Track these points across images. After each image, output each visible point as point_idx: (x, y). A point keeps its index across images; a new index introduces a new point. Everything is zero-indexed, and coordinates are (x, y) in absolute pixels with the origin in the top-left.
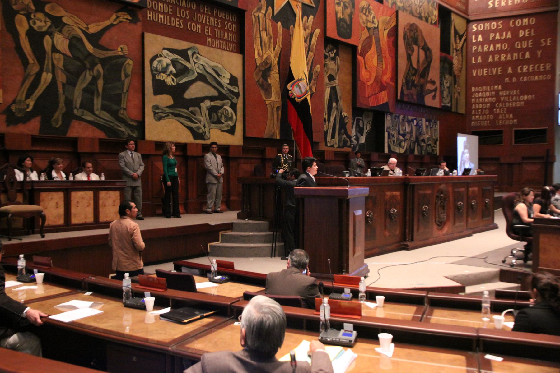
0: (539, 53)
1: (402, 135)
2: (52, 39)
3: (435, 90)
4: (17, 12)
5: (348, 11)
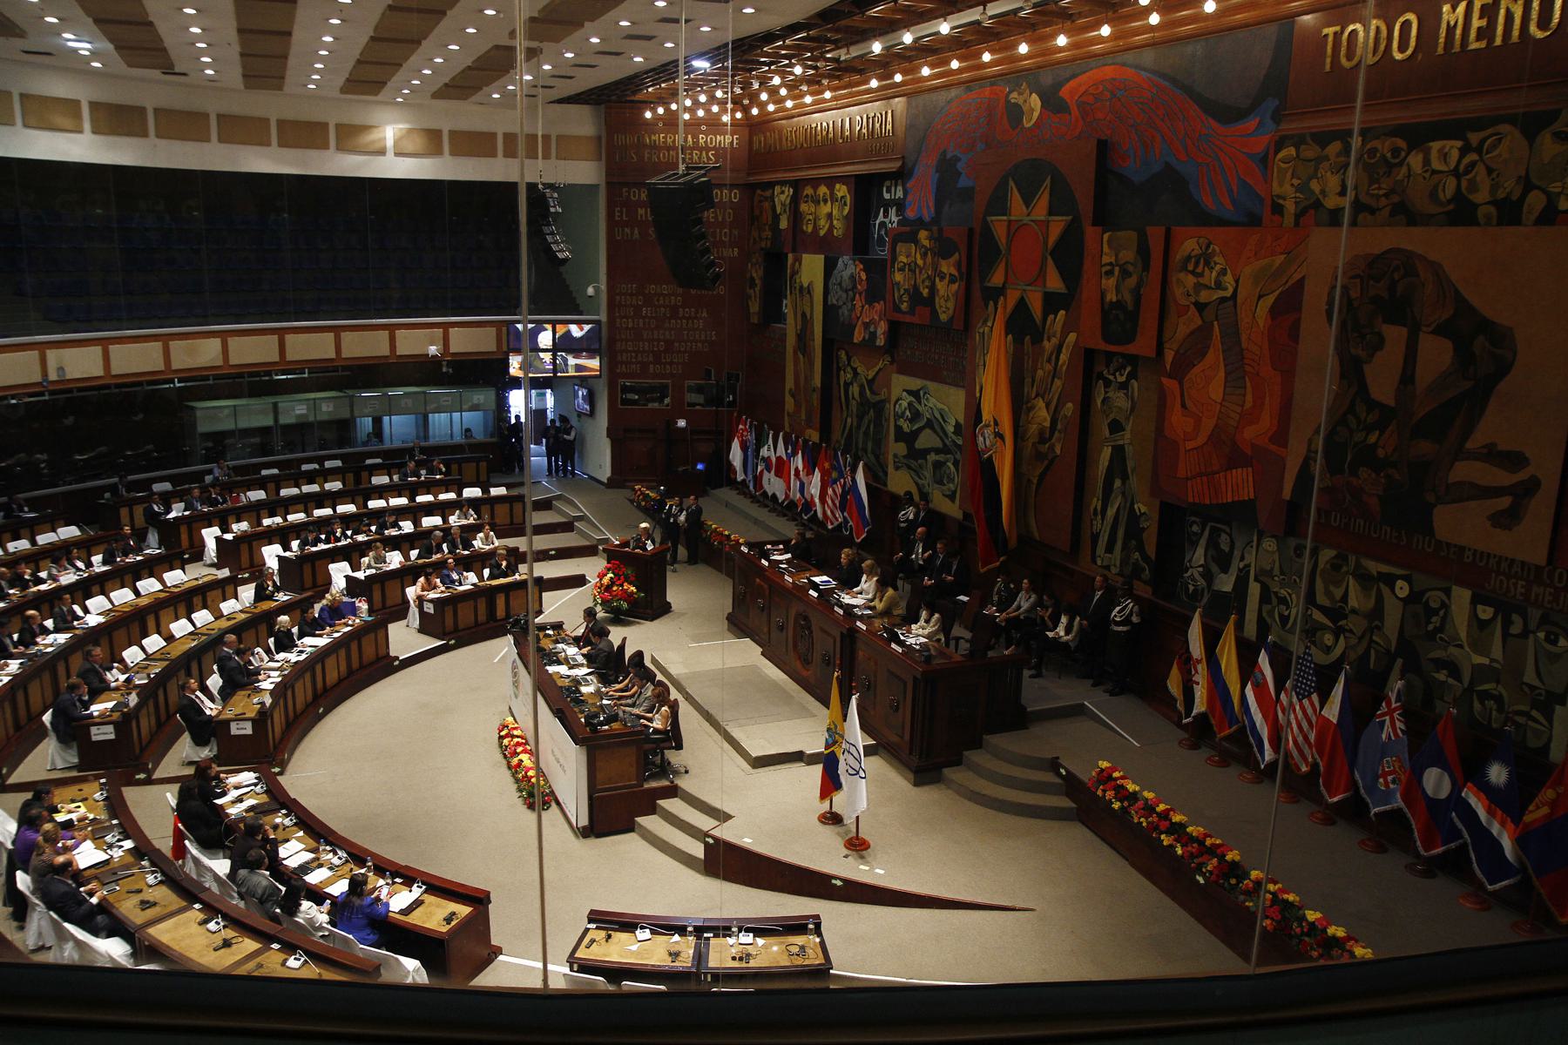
1: (1322, 609)
5: (1132, 282)
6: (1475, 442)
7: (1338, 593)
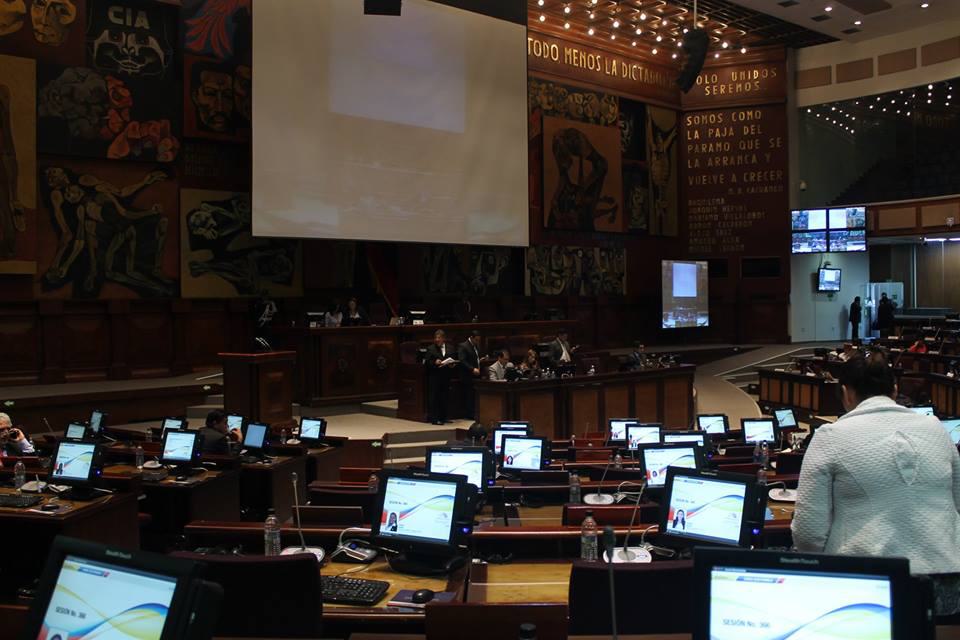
0: (768, 156)
1: (556, 271)
2: (85, 208)
3: (616, 207)
4: (53, 189)
6: (601, 197)
7: (560, 262)
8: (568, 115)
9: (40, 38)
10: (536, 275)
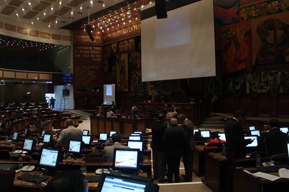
7: (266, 79)
8: (269, 13)
9: (130, 49)
10: (252, 85)
